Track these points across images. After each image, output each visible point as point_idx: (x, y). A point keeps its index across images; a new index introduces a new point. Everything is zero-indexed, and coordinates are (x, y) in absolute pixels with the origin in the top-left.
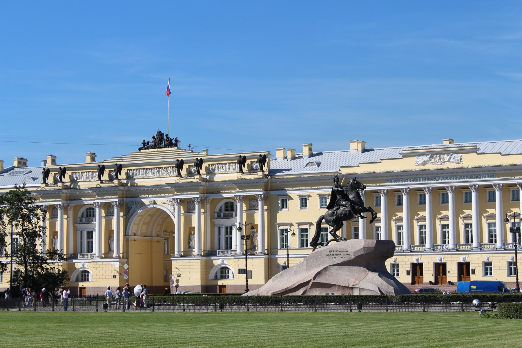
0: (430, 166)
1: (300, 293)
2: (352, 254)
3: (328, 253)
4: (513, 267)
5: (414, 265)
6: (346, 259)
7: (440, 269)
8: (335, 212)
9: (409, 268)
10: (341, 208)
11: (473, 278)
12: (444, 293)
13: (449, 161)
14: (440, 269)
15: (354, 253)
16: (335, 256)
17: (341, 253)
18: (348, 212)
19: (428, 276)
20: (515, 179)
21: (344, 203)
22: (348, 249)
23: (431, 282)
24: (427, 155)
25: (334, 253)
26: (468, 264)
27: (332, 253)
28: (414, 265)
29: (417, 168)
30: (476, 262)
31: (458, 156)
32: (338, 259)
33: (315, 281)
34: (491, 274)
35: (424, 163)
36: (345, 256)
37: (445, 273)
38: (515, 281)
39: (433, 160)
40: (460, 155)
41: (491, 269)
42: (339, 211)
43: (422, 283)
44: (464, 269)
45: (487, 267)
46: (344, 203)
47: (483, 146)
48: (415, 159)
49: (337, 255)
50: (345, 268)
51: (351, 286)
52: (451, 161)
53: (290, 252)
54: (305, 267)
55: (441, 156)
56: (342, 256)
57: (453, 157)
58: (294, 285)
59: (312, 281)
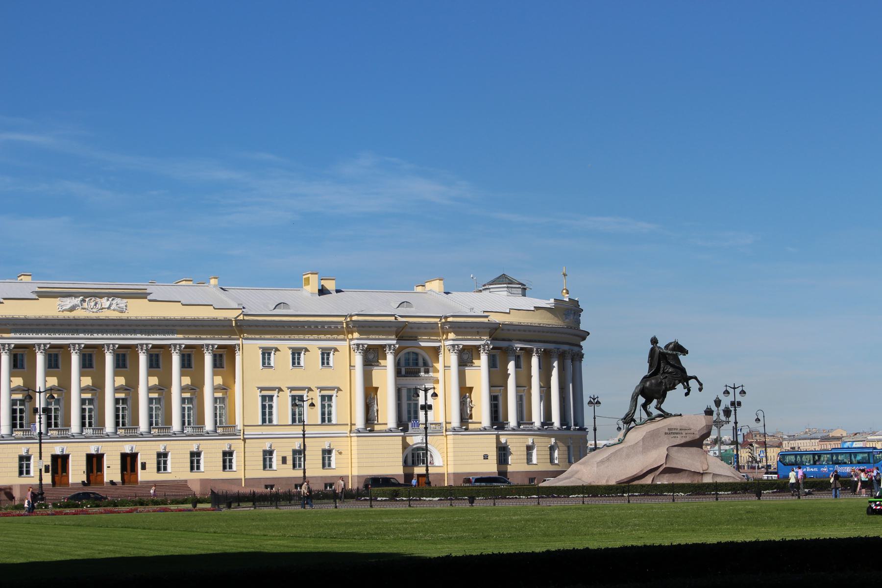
0: (79, 314)
1: (648, 480)
4: (327, 456)
6: (688, 439)
7: (95, 462)
9: (49, 463)
13: (109, 308)
14: (95, 462)
19: (77, 474)
20: (200, 339)
22: (692, 427)
23: (83, 482)
24: (76, 297)
26: (134, 456)
27: (671, 432)
30: (147, 452)
31: (122, 302)
33: (668, 466)
35: (72, 309)
37: (100, 468)
38: (302, 475)
39: (85, 305)
40: (125, 300)
43: (68, 483)
45: (162, 457)
47: (156, 291)
48: (57, 301)
50: (684, 449)
52: (112, 308)
53: (308, 430)
55: (98, 300)
56: (684, 435)
57: (114, 302)
59: (664, 466)
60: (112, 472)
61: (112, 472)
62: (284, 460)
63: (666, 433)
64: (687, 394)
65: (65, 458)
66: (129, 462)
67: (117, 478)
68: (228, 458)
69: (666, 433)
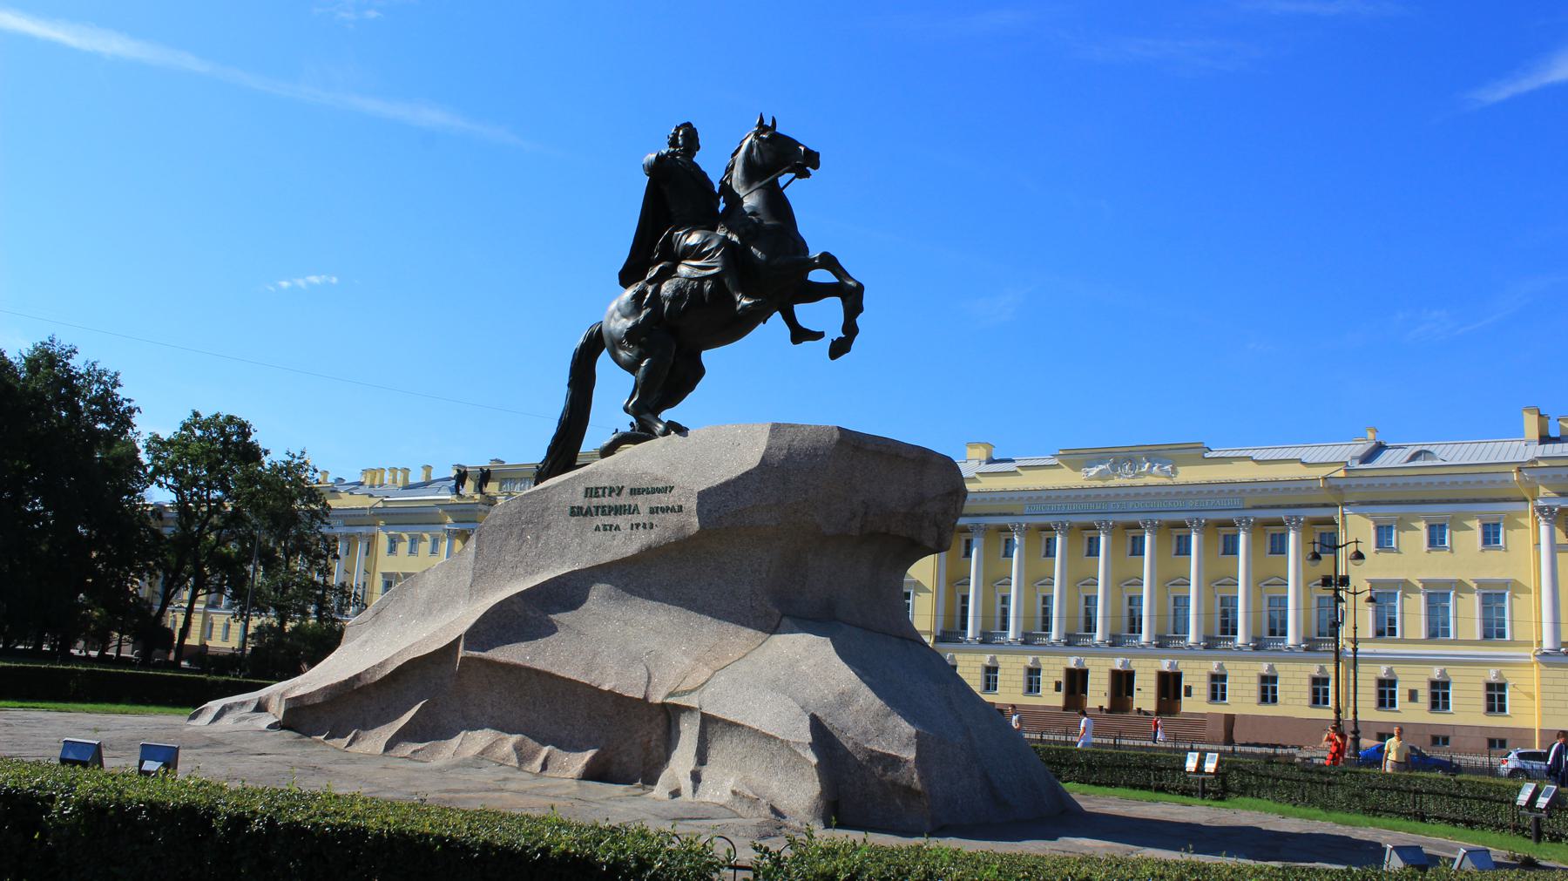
2: (692, 504)
3: (580, 501)
5: (1070, 673)
7: (1122, 683)
8: (650, 289)
9: (1061, 678)
10: (683, 270)
11: (1187, 705)
12: (1191, 764)
14: (1122, 683)
15: (703, 496)
16: (608, 520)
17: (640, 500)
18: (707, 287)
21: (694, 239)
22: (675, 479)
23: (1101, 708)
25: (606, 501)
26: (1178, 677)
27: (601, 506)
28: (1070, 673)
29: (1087, 484)
30: (1195, 674)
32: (620, 536)
34: (1224, 697)
36: (656, 519)
41: (1224, 688)
42: (667, 288)
44: (1170, 686)
46: (694, 239)
49: (618, 510)
51: (657, 698)
54: (467, 578)
58: (381, 665)
60: (1145, 697)
61: (1145, 697)
62: (1413, 696)
63: (576, 512)
64: (839, 348)
65: (1084, 674)
66: (1170, 686)
67: (1105, 703)
68: (1219, 684)
69: (576, 512)
